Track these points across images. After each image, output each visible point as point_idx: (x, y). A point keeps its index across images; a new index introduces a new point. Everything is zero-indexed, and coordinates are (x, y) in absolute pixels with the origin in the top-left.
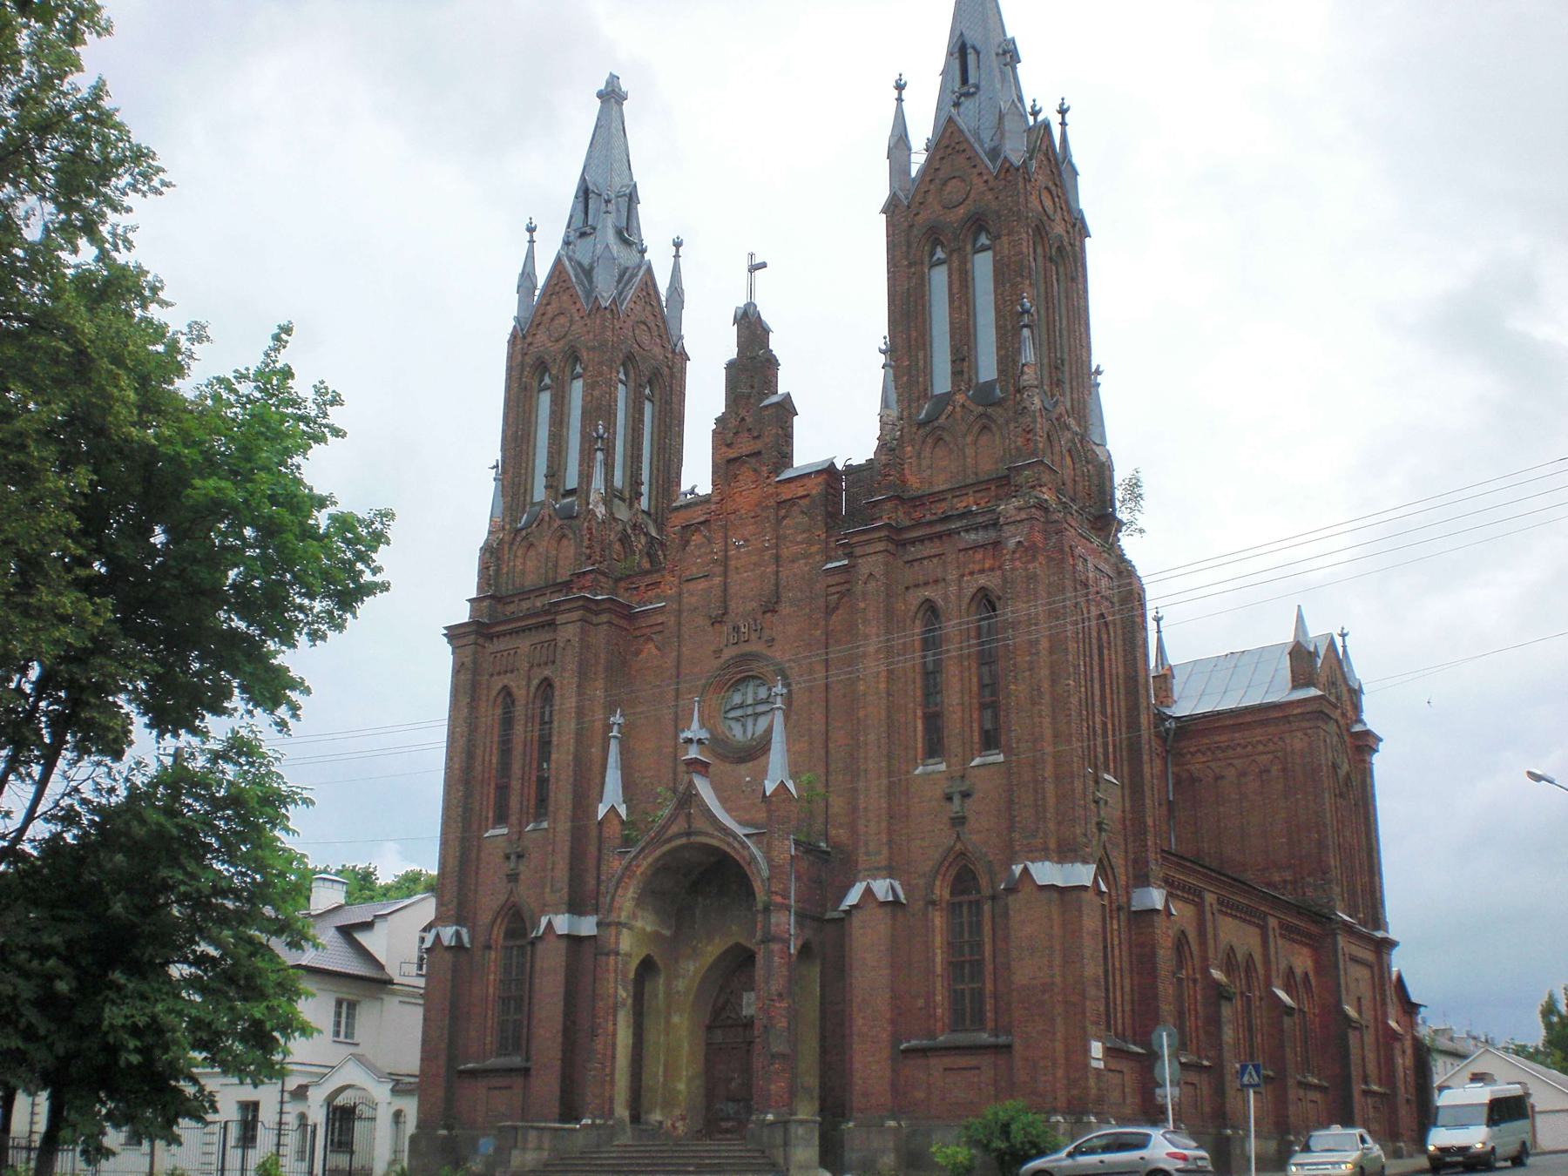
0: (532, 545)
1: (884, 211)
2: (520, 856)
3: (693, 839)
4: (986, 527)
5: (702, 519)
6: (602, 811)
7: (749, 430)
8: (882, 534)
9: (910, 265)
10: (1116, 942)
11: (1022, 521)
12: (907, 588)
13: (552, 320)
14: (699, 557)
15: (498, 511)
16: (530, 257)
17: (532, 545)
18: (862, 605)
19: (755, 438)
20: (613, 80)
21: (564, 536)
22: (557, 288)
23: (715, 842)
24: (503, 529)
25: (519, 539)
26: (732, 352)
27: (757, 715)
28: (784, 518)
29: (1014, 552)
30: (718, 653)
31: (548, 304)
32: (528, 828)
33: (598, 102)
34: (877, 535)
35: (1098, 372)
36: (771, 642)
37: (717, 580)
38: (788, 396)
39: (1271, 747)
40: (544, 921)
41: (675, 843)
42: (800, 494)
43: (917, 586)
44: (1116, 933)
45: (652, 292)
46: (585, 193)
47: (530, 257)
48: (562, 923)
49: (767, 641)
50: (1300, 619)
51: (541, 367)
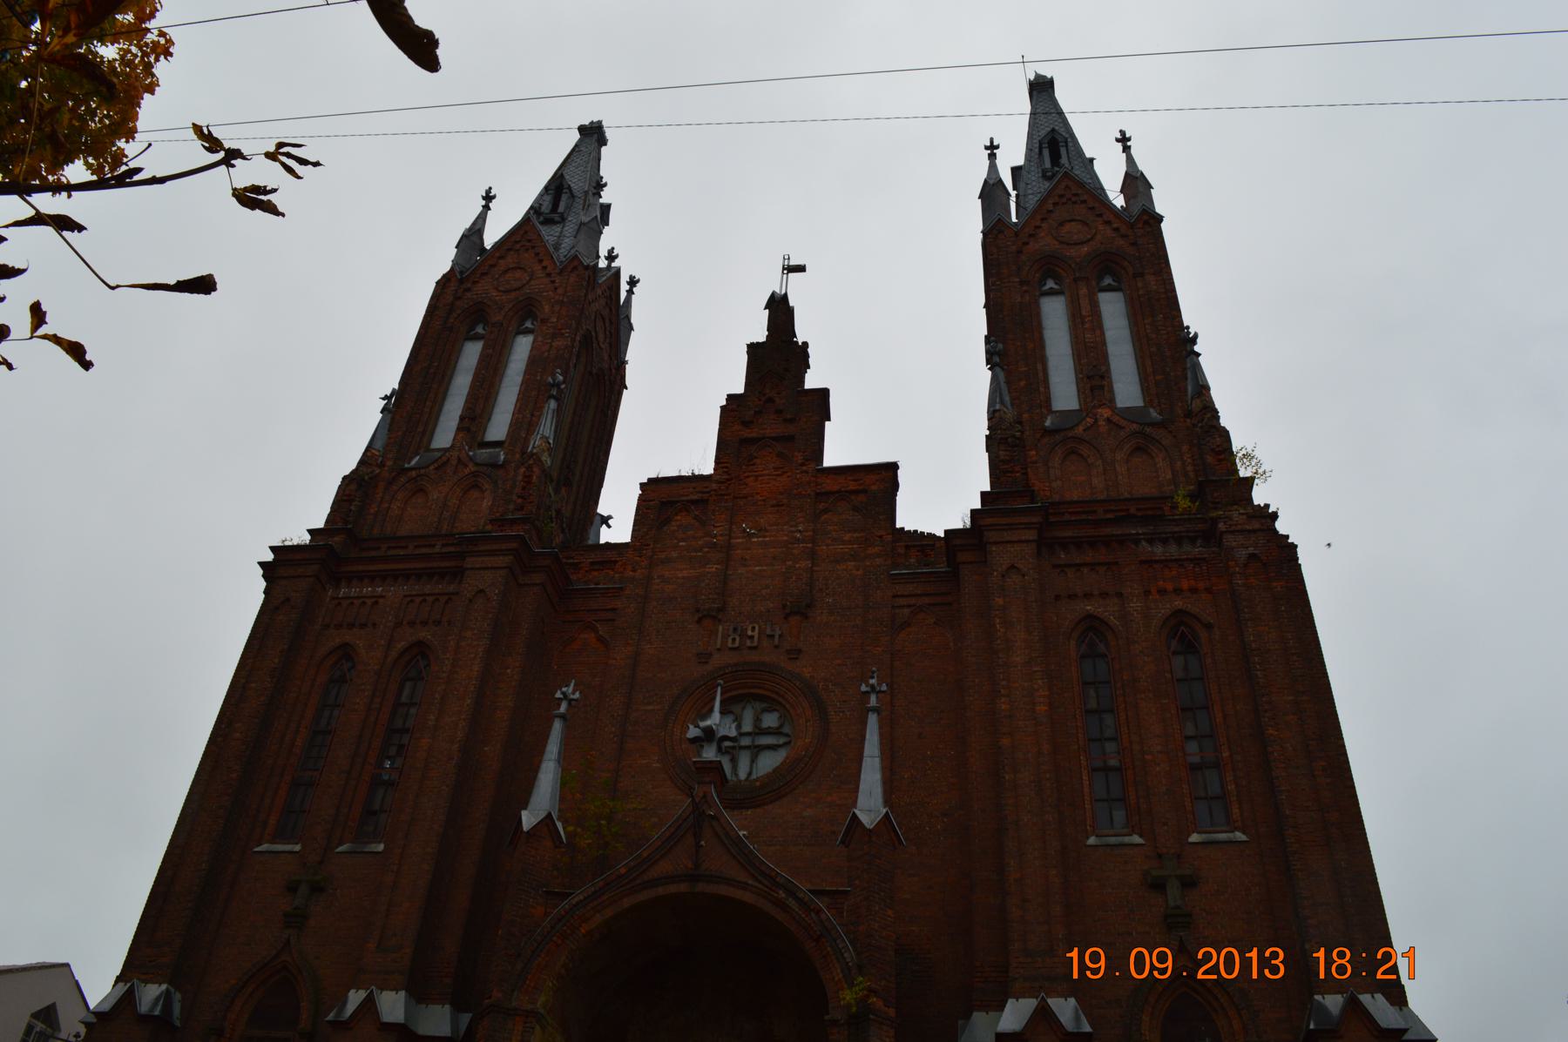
0: (422, 490)
2: (317, 889)
3: (701, 887)
4: (1179, 540)
5: (695, 497)
6: (528, 820)
7: (779, 412)
8: (1034, 520)
9: (1022, 283)
11: (1254, 531)
12: (1057, 597)
13: (506, 272)
14: (683, 540)
15: (379, 445)
16: (481, 220)
17: (422, 490)
18: (1000, 601)
19: (785, 420)
21: (476, 486)
22: (518, 246)
23: (747, 897)
24: (382, 465)
25: (403, 479)
26: (761, 335)
27: (756, 750)
28: (825, 511)
29: (1245, 565)
30: (703, 657)
31: (501, 257)
32: (340, 849)
34: (1024, 520)
36: (795, 654)
37: (712, 568)
38: (824, 394)
40: (355, 998)
41: (661, 891)
42: (851, 488)
43: (1072, 597)
45: (614, 297)
46: (557, 186)
47: (481, 220)
48: (393, 1006)
49: (788, 652)
51: (478, 313)
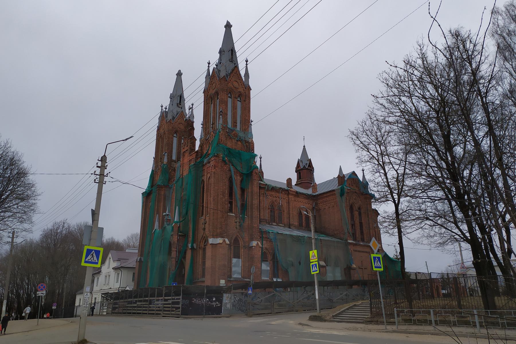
1: (203, 93)
10: (243, 254)
20: (180, 71)
33: (176, 76)
35: (252, 121)
39: (334, 201)
44: (242, 253)
50: (340, 169)
